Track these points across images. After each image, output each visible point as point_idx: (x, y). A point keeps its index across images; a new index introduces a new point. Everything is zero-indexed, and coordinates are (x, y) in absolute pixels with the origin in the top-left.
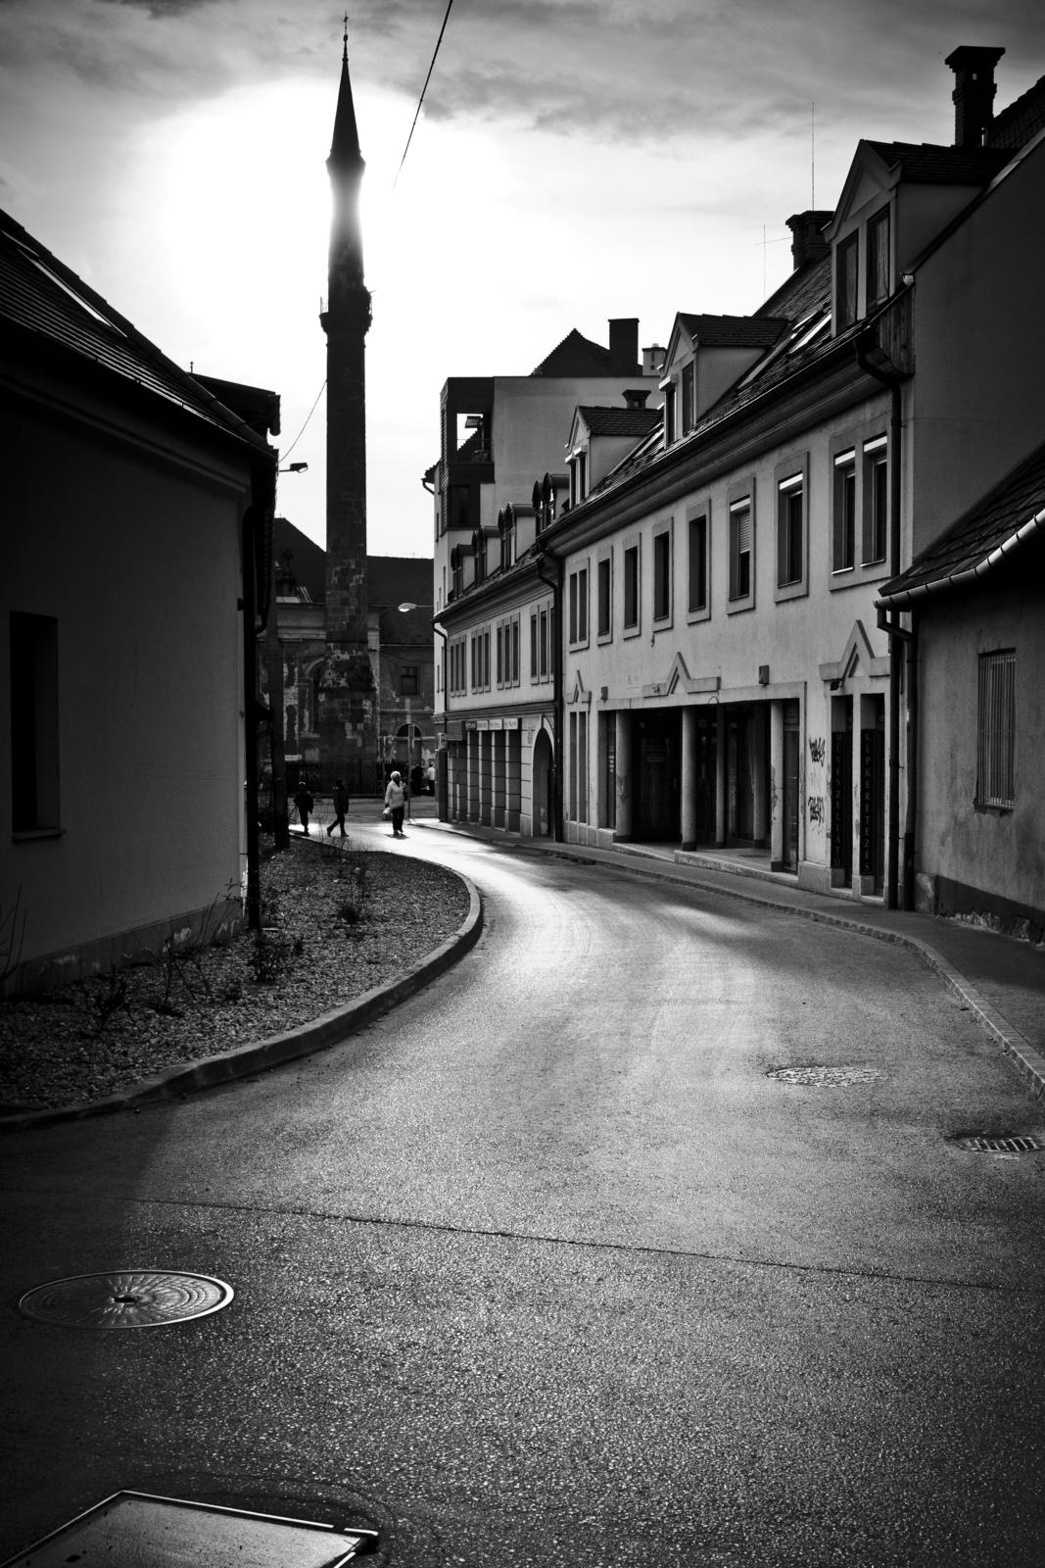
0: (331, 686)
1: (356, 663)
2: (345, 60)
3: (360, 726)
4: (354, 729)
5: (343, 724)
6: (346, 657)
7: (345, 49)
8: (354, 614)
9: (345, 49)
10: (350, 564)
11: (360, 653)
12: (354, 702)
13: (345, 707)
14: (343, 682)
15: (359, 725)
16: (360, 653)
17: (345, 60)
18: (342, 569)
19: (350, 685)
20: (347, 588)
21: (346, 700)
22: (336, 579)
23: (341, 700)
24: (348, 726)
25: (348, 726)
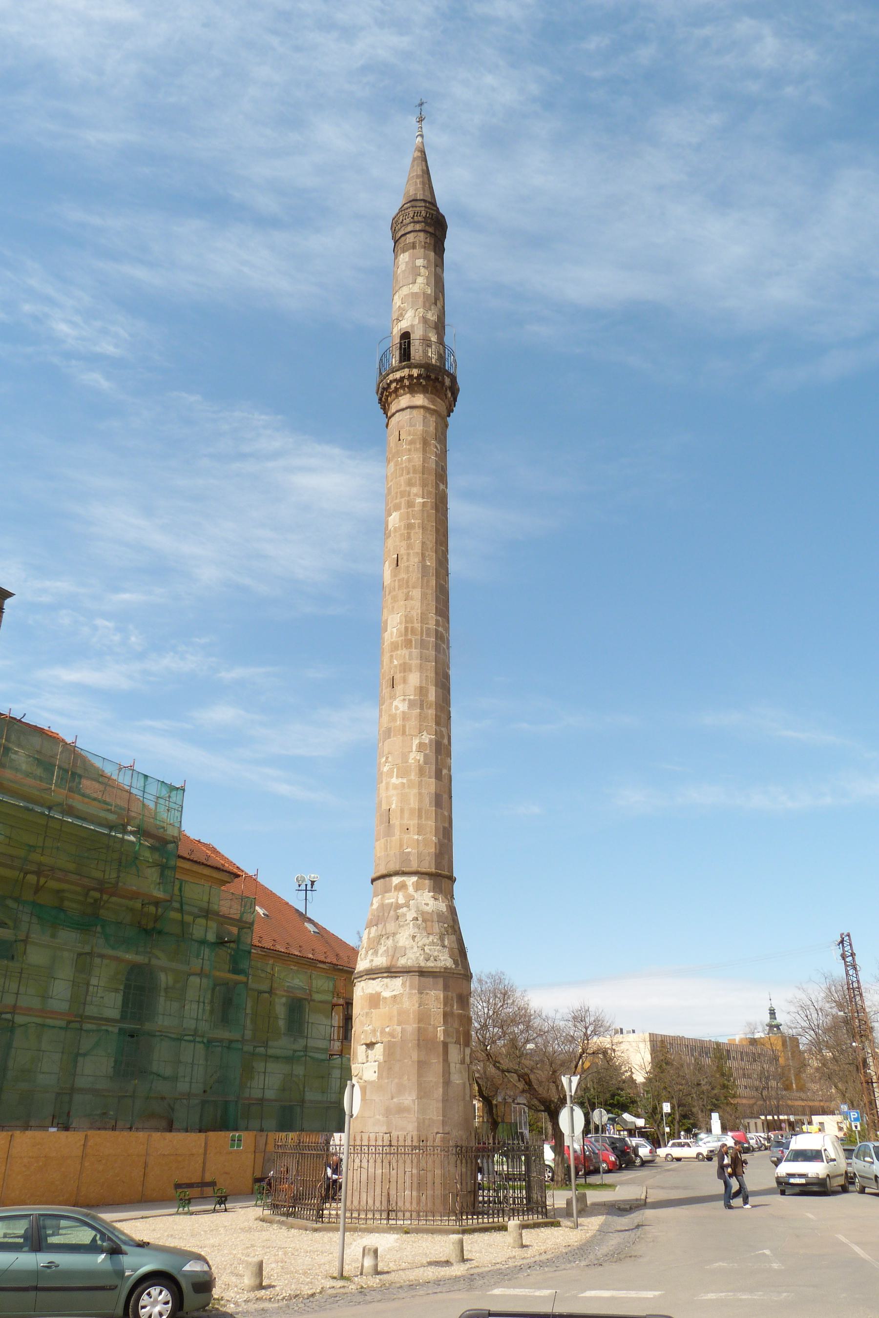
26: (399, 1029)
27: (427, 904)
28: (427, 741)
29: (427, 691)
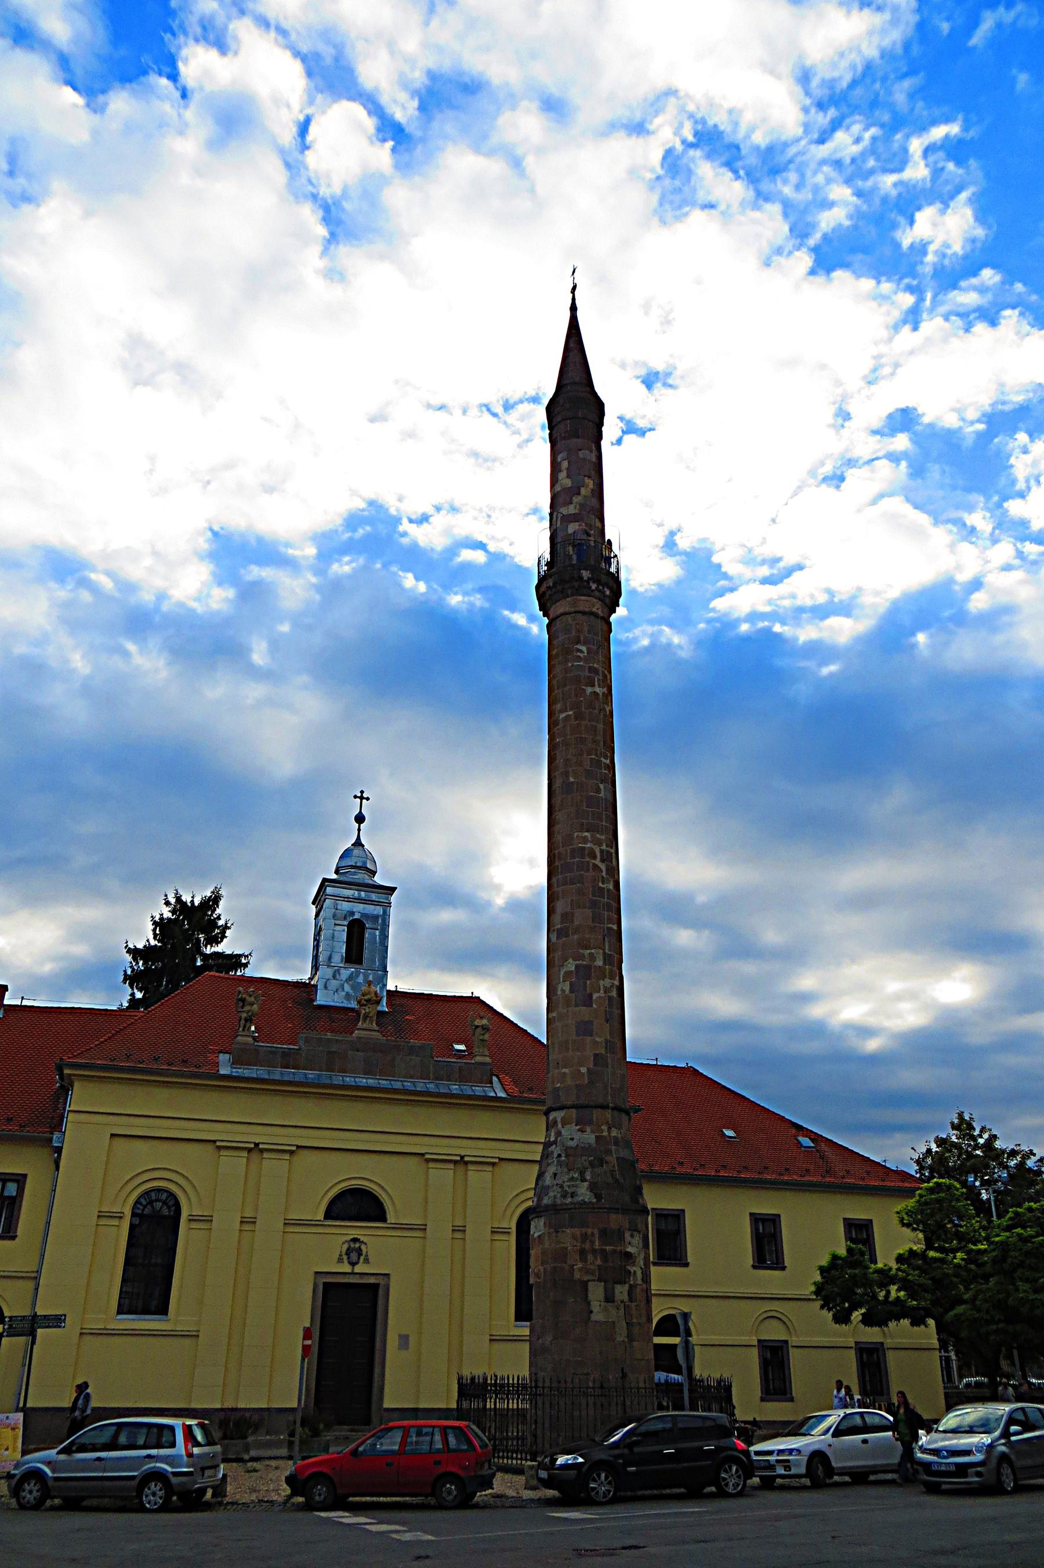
0: (558, 1201)
1: (609, 1152)
2: (573, 308)
3: (621, 1292)
4: (609, 1298)
5: (585, 1285)
6: (590, 1138)
7: (574, 299)
8: (603, 1051)
9: (574, 299)
10: (592, 957)
11: (614, 1133)
12: (605, 1234)
13: (587, 1246)
14: (584, 1193)
15: (618, 1288)
16: (614, 1133)
17: (573, 308)
18: (577, 966)
19: (598, 1197)
20: (588, 1001)
21: (589, 1231)
22: (567, 987)
23: (577, 1231)
24: (596, 1292)
25: (596, 1292)
26: (542, 1269)
27: (572, 1139)
28: (573, 968)
29: (573, 914)
